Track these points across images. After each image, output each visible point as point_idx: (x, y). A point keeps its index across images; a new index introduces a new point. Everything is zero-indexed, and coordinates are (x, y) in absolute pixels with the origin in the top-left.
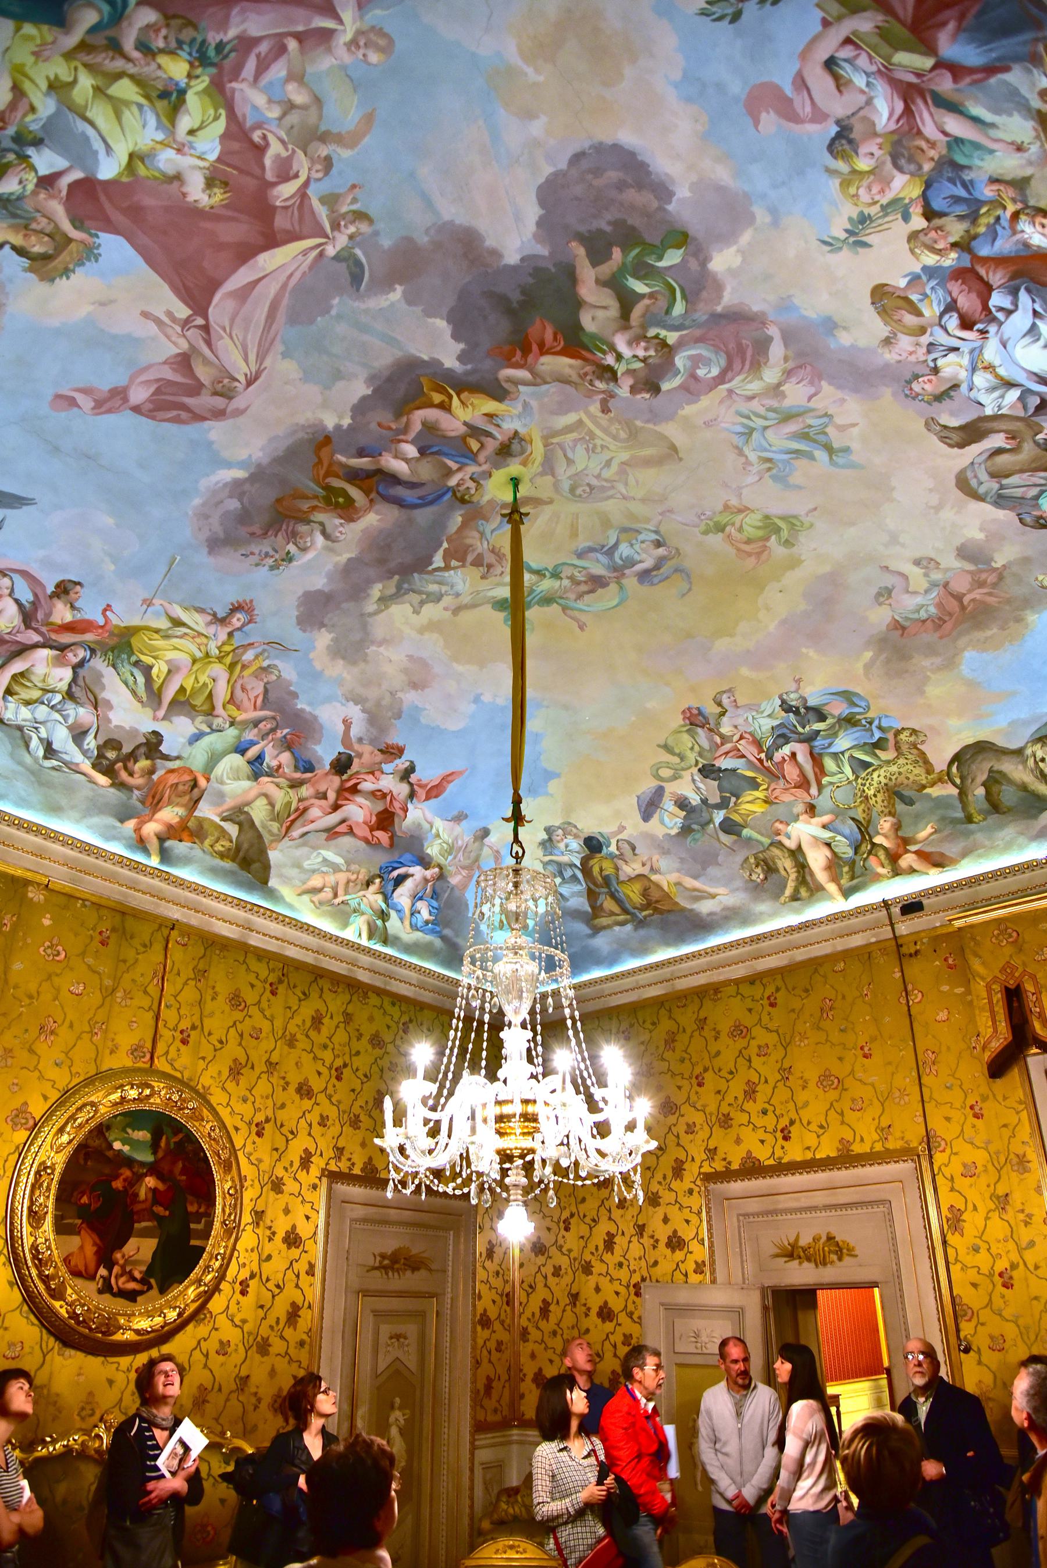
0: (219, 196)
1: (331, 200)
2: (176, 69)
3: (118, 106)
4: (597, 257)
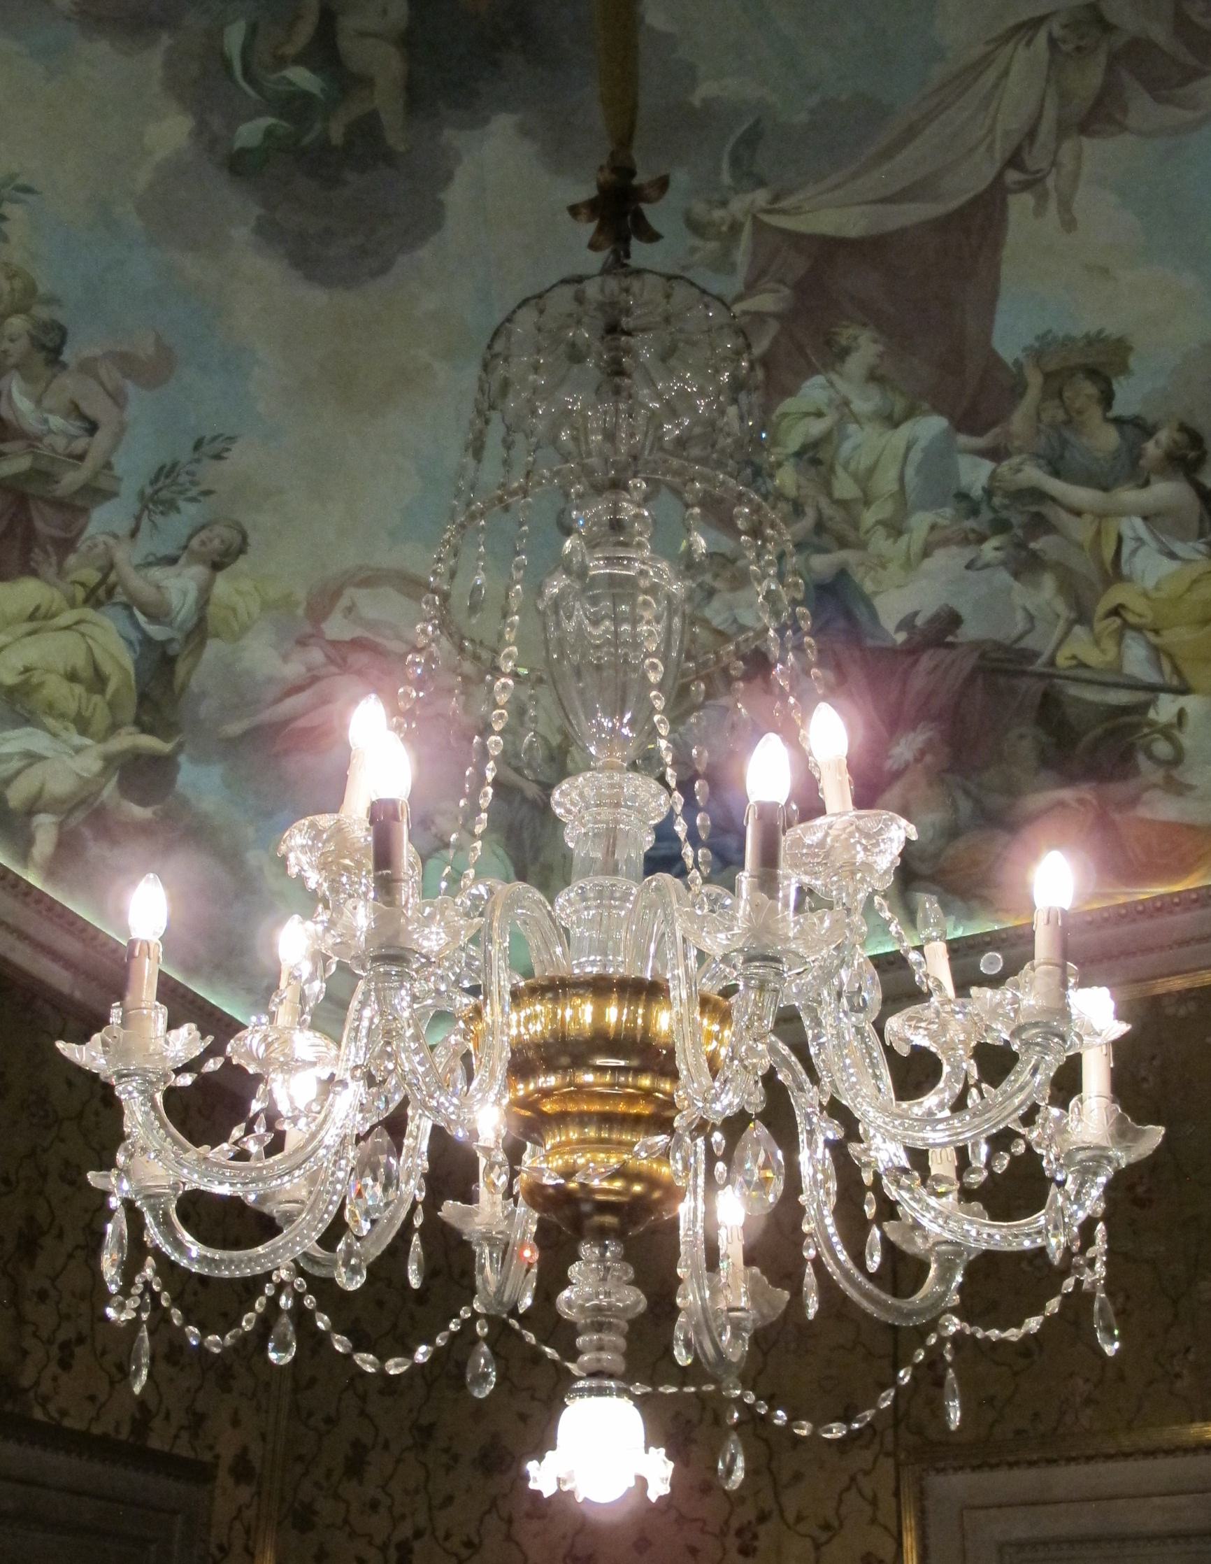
0: (845, 334)
1: (723, 264)
2: (786, 479)
3: (864, 479)
4: (368, 128)
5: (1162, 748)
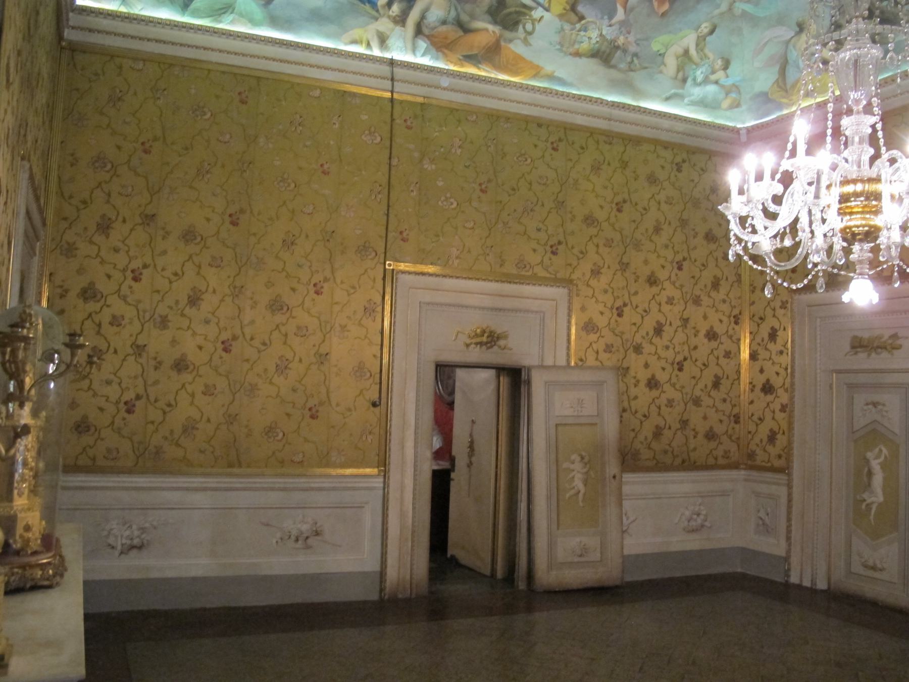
5: (529, 27)
